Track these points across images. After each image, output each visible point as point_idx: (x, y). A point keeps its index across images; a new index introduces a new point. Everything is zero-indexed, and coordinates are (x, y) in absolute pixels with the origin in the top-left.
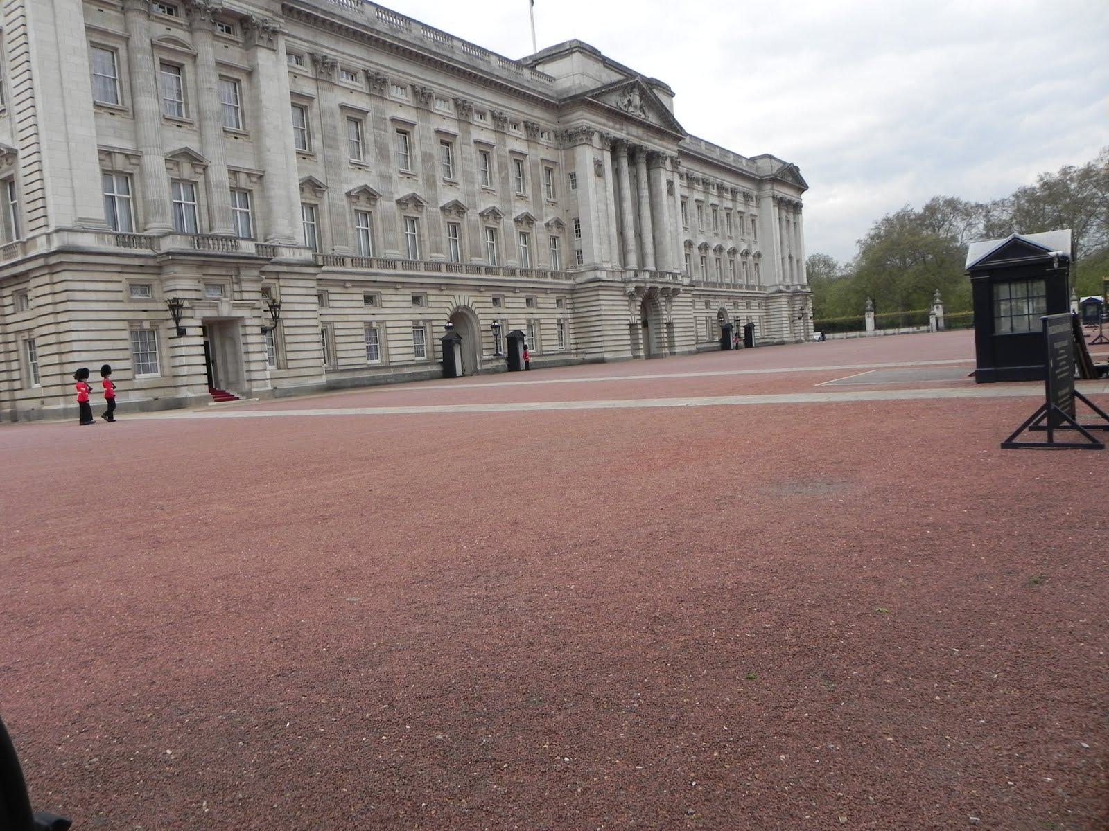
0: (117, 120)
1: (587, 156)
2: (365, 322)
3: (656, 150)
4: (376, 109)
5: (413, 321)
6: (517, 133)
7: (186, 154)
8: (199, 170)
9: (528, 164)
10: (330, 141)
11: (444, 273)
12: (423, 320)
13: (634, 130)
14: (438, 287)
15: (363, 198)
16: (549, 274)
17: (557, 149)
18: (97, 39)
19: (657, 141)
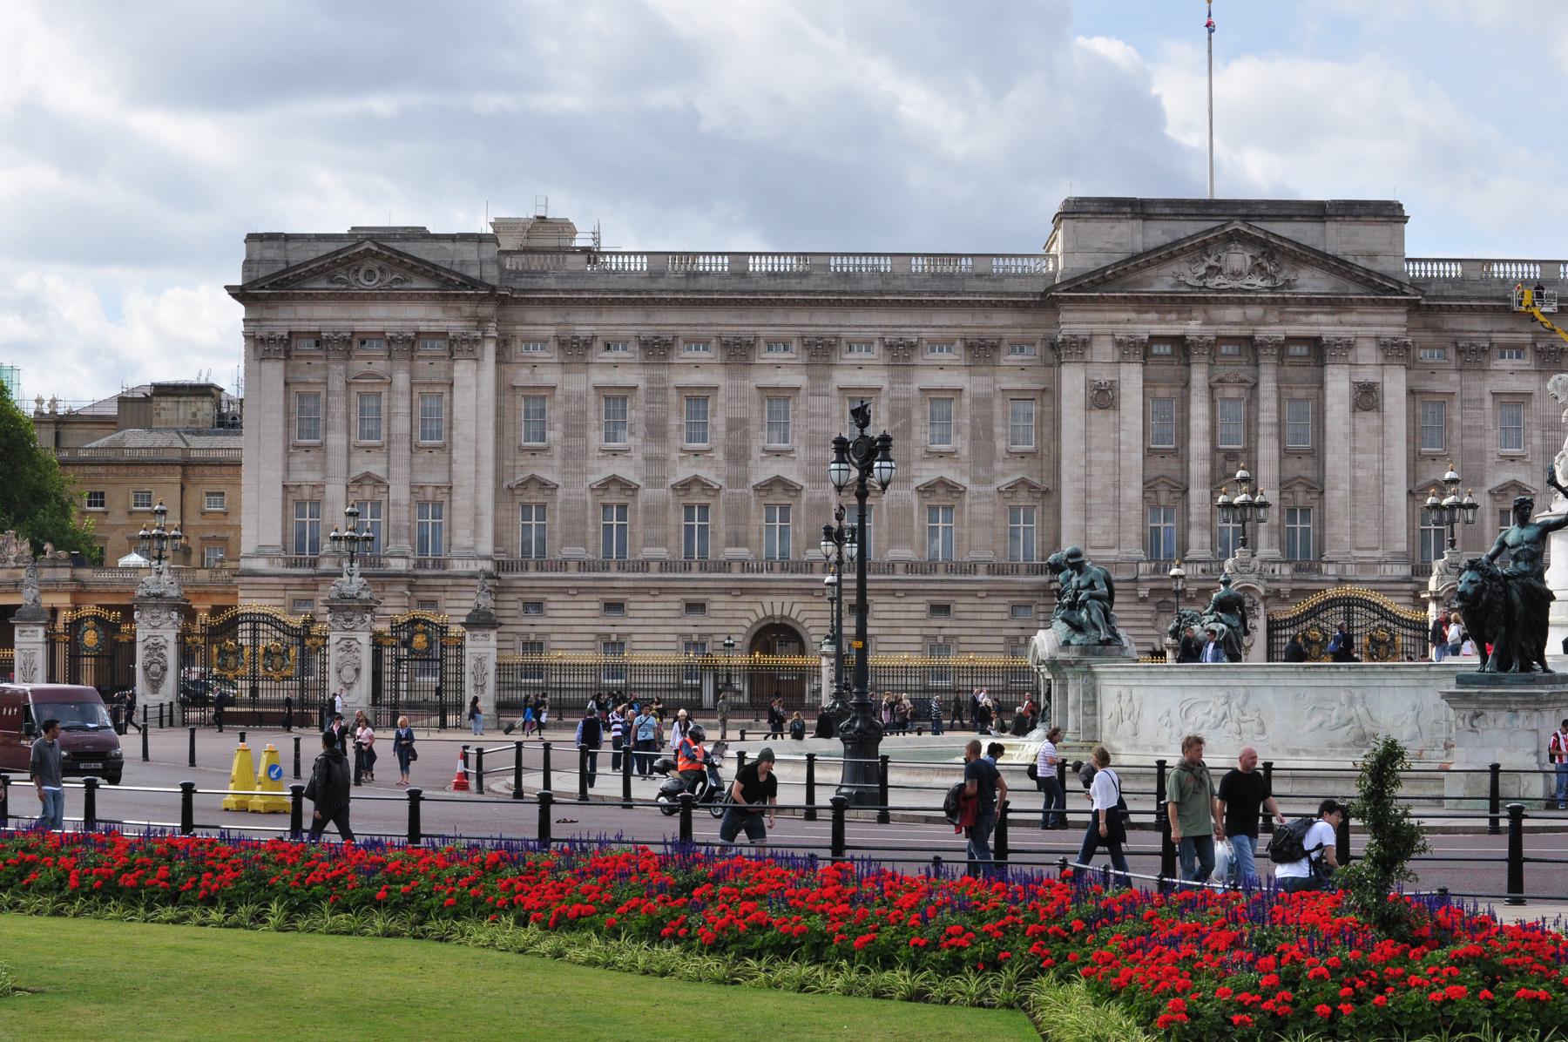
0: (311, 456)
1: (1073, 381)
2: (599, 634)
3: (1316, 334)
4: (649, 380)
5: (680, 635)
6: (944, 357)
7: (368, 475)
8: (383, 490)
9: (966, 401)
10: (575, 428)
11: (736, 574)
12: (700, 635)
13: (1233, 313)
14: (727, 591)
15: (614, 488)
16: (981, 567)
17: (1051, 366)
18: (302, 389)
19: (1322, 318)
